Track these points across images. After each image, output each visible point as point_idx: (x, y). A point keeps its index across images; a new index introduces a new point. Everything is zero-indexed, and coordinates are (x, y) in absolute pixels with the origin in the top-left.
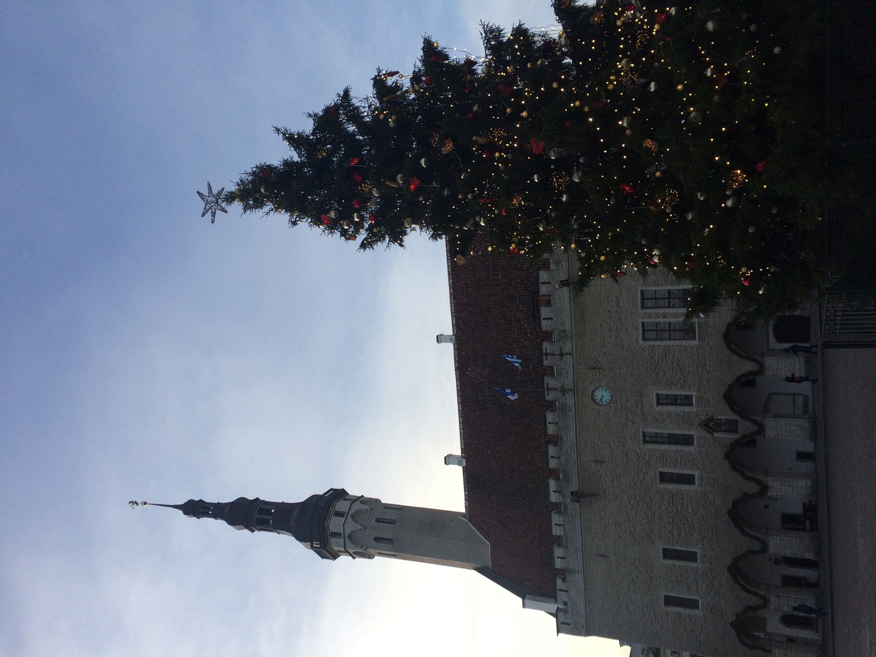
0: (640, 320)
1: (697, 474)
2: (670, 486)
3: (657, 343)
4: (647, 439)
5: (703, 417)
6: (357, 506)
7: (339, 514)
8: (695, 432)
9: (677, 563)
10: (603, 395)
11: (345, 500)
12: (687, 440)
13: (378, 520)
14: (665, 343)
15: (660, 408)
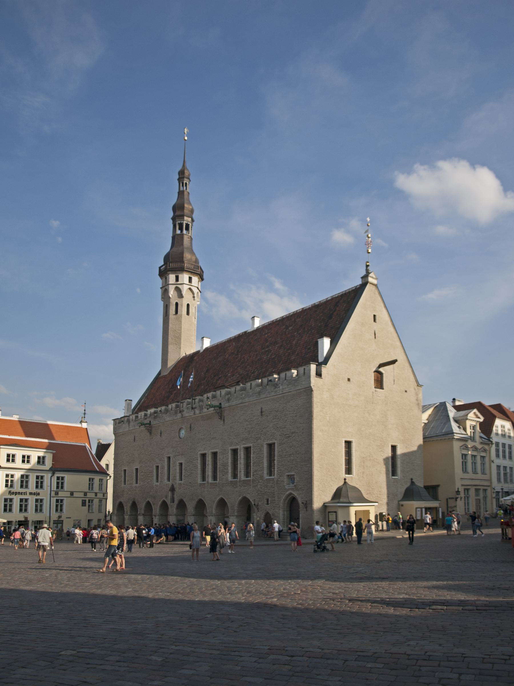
0: (206, 452)
1: (158, 484)
2: (155, 471)
3: (199, 461)
4: (169, 458)
5: (175, 486)
6: (185, 289)
7: (177, 279)
8: (170, 483)
9: (135, 474)
10: (183, 433)
11: (190, 279)
12: (169, 479)
13: (177, 304)
14: (199, 466)
15: (178, 464)
